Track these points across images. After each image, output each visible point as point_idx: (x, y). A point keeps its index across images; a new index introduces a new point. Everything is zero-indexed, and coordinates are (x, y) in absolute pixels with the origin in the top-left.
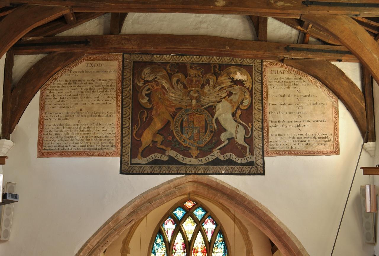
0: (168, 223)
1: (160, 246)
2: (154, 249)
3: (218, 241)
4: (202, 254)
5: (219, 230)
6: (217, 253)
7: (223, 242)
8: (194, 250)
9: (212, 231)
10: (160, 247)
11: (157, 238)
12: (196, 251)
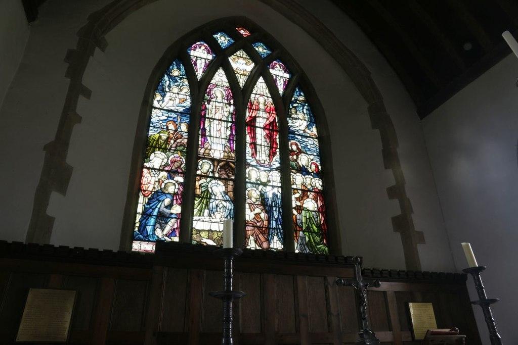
0: (197, 50)
1: (178, 82)
2: (163, 85)
3: (296, 100)
4: (268, 114)
5: (298, 81)
6: (296, 119)
7: (307, 105)
8: (252, 105)
9: (284, 82)
10: (176, 84)
11: (171, 67)
12: (254, 107)
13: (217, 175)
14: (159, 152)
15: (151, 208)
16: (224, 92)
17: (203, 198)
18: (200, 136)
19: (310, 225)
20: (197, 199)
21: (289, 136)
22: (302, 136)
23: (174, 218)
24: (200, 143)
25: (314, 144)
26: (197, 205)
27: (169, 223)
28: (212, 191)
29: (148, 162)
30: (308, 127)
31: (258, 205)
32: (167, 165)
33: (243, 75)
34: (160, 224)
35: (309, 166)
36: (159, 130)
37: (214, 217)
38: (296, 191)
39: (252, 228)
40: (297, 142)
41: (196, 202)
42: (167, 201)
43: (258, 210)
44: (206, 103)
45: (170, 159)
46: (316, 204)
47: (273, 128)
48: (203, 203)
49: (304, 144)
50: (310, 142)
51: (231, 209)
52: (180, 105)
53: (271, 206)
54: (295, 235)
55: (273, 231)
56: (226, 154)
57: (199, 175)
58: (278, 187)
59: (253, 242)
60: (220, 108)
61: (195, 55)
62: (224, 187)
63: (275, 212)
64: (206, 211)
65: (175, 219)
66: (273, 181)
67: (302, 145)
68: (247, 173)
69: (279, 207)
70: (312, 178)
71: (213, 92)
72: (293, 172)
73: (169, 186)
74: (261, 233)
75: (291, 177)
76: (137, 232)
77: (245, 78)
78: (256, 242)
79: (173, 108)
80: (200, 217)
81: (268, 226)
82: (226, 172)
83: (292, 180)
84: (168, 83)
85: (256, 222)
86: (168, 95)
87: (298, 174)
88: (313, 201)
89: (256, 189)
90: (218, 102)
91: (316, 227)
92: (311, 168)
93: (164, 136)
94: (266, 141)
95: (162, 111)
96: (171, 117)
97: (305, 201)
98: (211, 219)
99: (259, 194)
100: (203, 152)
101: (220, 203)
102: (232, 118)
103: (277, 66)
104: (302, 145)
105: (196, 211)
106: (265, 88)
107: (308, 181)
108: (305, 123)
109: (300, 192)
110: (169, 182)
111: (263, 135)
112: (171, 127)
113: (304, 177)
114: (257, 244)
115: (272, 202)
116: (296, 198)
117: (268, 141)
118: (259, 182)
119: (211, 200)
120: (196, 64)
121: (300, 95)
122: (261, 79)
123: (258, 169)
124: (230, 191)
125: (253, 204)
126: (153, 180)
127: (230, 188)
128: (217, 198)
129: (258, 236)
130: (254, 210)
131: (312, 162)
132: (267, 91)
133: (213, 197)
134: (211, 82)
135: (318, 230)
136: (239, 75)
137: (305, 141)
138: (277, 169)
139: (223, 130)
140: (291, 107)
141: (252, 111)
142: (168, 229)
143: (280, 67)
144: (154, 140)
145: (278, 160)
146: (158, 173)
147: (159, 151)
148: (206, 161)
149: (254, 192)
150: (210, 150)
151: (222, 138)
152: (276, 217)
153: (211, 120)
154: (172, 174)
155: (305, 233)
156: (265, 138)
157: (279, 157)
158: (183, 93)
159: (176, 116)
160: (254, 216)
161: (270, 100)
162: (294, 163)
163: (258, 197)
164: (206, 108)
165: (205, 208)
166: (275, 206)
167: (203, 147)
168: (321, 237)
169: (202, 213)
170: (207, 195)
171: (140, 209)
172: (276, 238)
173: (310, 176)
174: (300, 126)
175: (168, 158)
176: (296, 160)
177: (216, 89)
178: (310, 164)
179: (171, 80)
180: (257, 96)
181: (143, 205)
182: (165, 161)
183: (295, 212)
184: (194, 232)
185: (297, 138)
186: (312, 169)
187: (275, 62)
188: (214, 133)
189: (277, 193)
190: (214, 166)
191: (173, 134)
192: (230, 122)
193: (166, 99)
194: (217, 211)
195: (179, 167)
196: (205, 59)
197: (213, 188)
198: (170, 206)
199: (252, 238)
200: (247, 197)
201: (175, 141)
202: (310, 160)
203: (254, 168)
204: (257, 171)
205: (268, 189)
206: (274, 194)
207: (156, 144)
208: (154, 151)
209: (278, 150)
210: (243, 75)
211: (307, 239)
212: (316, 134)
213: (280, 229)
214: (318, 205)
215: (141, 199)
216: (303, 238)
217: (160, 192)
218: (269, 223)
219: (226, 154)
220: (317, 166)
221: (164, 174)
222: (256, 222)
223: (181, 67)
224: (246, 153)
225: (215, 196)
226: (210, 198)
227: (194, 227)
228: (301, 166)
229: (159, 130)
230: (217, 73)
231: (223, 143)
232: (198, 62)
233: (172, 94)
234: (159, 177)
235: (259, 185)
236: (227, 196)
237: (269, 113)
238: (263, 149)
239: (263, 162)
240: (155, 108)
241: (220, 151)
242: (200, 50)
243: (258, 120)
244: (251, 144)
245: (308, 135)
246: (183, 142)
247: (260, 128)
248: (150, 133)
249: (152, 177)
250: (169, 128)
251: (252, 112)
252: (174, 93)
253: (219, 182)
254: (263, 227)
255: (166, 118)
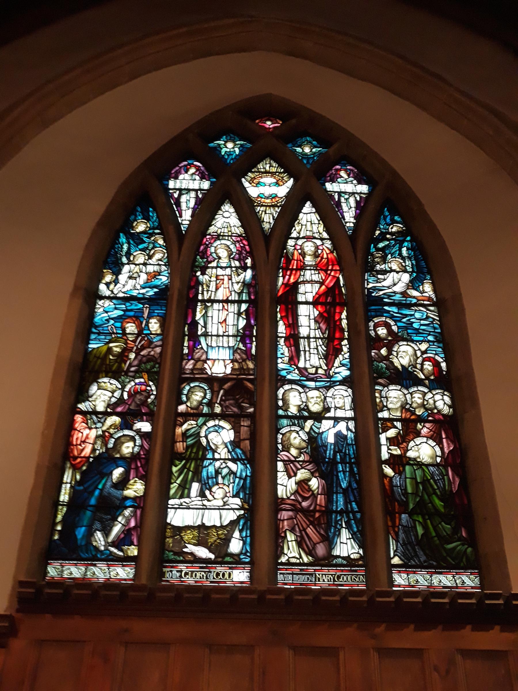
1: (145, 242)
6: (384, 272)
7: (408, 238)
8: (289, 261)
9: (357, 202)
10: (141, 247)
13: (218, 410)
14: (106, 380)
15: (85, 489)
16: (232, 247)
17: (188, 460)
18: (186, 338)
19: (426, 497)
20: (177, 462)
21: (370, 311)
22: (400, 305)
23: (130, 507)
24: (186, 351)
25: (427, 317)
26: (176, 475)
27: (120, 519)
28: (208, 442)
29: (84, 401)
30: (413, 284)
31: (303, 461)
32: (121, 401)
33: (270, 206)
34: (101, 521)
35: (419, 366)
36: (109, 337)
37: (210, 497)
38: (389, 424)
39: (290, 513)
40: (388, 320)
41: (174, 469)
42: (117, 473)
43: (302, 474)
44: (199, 273)
45: (127, 389)
46: (437, 449)
47: (334, 299)
48: (189, 470)
49: (404, 320)
50: (418, 315)
51: (246, 476)
52: (148, 284)
53: (333, 462)
54: (390, 524)
55: (339, 518)
56: (237, 366)
57: (182, 414)
58: (348, 419)
59: (293, 545)
60: (226, 278)
61: (177, 187)
62: (232, 432)
63: (341, 475)
64: (195, 487)
65: (131, 509)
66: (336, 408)
67: (399, 324)
68: (280, 397)
69: (351, 464)
70: (426, 390)
71: (213, 250)
72: (380, 384)
73: (123, 443)
74: (312, 523)
75: (377, 395)
76: (58, 542)
77: (275, 212)
78: (300, 544)
79: (135, 293)
80: (182, 500)
81: (326, 506)
82: (237, 400)
83: (378, 400)
84: (125, 247)
85: (300, 499)
86: (126, 269)
87: (391, 387)
88: (431, 442)
89: (297, 429)
90: (221, 268)
91: (441, 500)
92: (422, 370)
93: (116, 348)
94: (319, 328)
95: (114, 301)
96: (131, 310)
97: (412, 444)
98: (206, 503)
99: (305, 437)
100: (191, 367)
101: (224, 465)
102: (249, 294)
103: (343, 173)
104: (399, 324)
105: (174, 487)
106: (317, 222)
107: (417, 398)
108: (406, 278)
109: (399, 425)
110: (124, 435)
111: (312, 317)
112: (131, 328)
113: (406, 392)
114: (304, 550)
115: (335, 453)
116: (388, 439)
117: (323, 326)
118: (306, 414)
119: (206, 463)
120: (178, 203)
121: (393, 222)
122: (308, 207)
123: (303, 386)
124: (244, 440)
125: (292, 462)
126: (93, 434)
127: (244, 431)
128: (217, 456)
129: (305, 530)
130: (295, 475)
131: (424, 356)
132: (321, 228)
133: (210, 456)
134: (209, 232)
135: (444, 507)
136: (263, 209)
137: (406, 316)
138: (344, 382)
139: (231, 320)
140: (373, 250)
141: (288, 273)
142: (116, 529)
143: (349, 175)
144: (98, 358)
145: (346, 362)
146: (102, 420)
147: (106, 376)
148: (197, 384)
149: (294, 435)
150: (205, 361)
151: (228, 336)
152: (344, 485)
153: (209, 304)
154: (129, 418)
155: (415, 517)
156: (316, 321)
157: (347, 356)
158: (154, 261)
159: (141, 306)
160: (294, 487)
161: (328, 244)
162: (383, 365)
163: (304, 444)
164: (199, 283)
165: (192, 481)
166: (343, 462)
167: (192, 359)
168: (453, 523)
169: (186, 491)
170: (197, 453)
171: (64, 497)
172: (345, 534)
173: (421, 388)
174: (395, 285)
175: (123, 389)
176: (387, 358)
177: (218, 242)
178: (419, 361)
179: (132, 242)
180: (300, 242)
181: (71, 487)
182: (117, 394)
183: (388, 471)
184: (169, 533)
185: (388, 312)
186: (426, 372)
187: (338, 167)
188: (212, 329)
189: (345, 432)
190: (212, 392)
191: (134, 341)
192: (245, 302)
193: (123, 278)
194: (217, 484)
195: (144, 403)
196: (196, 191)
197: (210, 437)
198: (123, 483)
199: (290, 537)
200: (280, 447)
201: (137, 354)
202: (419, 353)
203: (294, 386)
204: (301, 390)
205: (326, 424)
206: (339, 436)
207: (102, 364)
208: (95, 380)
209: (345, 342)
210: (270, 206)
211: (420, 531)
212: (433, 296)
213: (354, 513)
214: (442, 449)
215: (67, 477)
216: (410, 530)
217: (105, 458)
218: (329, 500)
219: (237, 366)
220: (436, 364)
221: (115, 420)
222: (300, 499)
223: (151, 214)
224: (277, 358)
225: (214, 451)
226: (204, 458)
227: (168, 521)
228: (400, 367)
229: (109, 337)
230: (220, 212)
231: (231, 344)
232: (184, 198)
233: (133, 266)
234: (104, 428)
235: (306, 419)
236: (238, 451)
237: (326, 271)
238: (313, 345)
239: (313, 371)
240: (102, 298)
241: (224, 360)
242: (187, 176)
243: (302, 288)
244: (286, 339)
245: (414, 301)
246: (152, 353)
247: (307, 303)
248: (90, 346)
249: (90, 428)
250: (128, 331)
251: (290, 276)
252: (136, 265)
253: (222, 423)
254: (315, 511)
255: (122, 313)
